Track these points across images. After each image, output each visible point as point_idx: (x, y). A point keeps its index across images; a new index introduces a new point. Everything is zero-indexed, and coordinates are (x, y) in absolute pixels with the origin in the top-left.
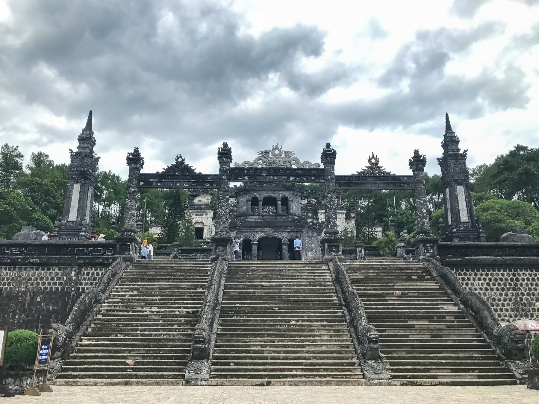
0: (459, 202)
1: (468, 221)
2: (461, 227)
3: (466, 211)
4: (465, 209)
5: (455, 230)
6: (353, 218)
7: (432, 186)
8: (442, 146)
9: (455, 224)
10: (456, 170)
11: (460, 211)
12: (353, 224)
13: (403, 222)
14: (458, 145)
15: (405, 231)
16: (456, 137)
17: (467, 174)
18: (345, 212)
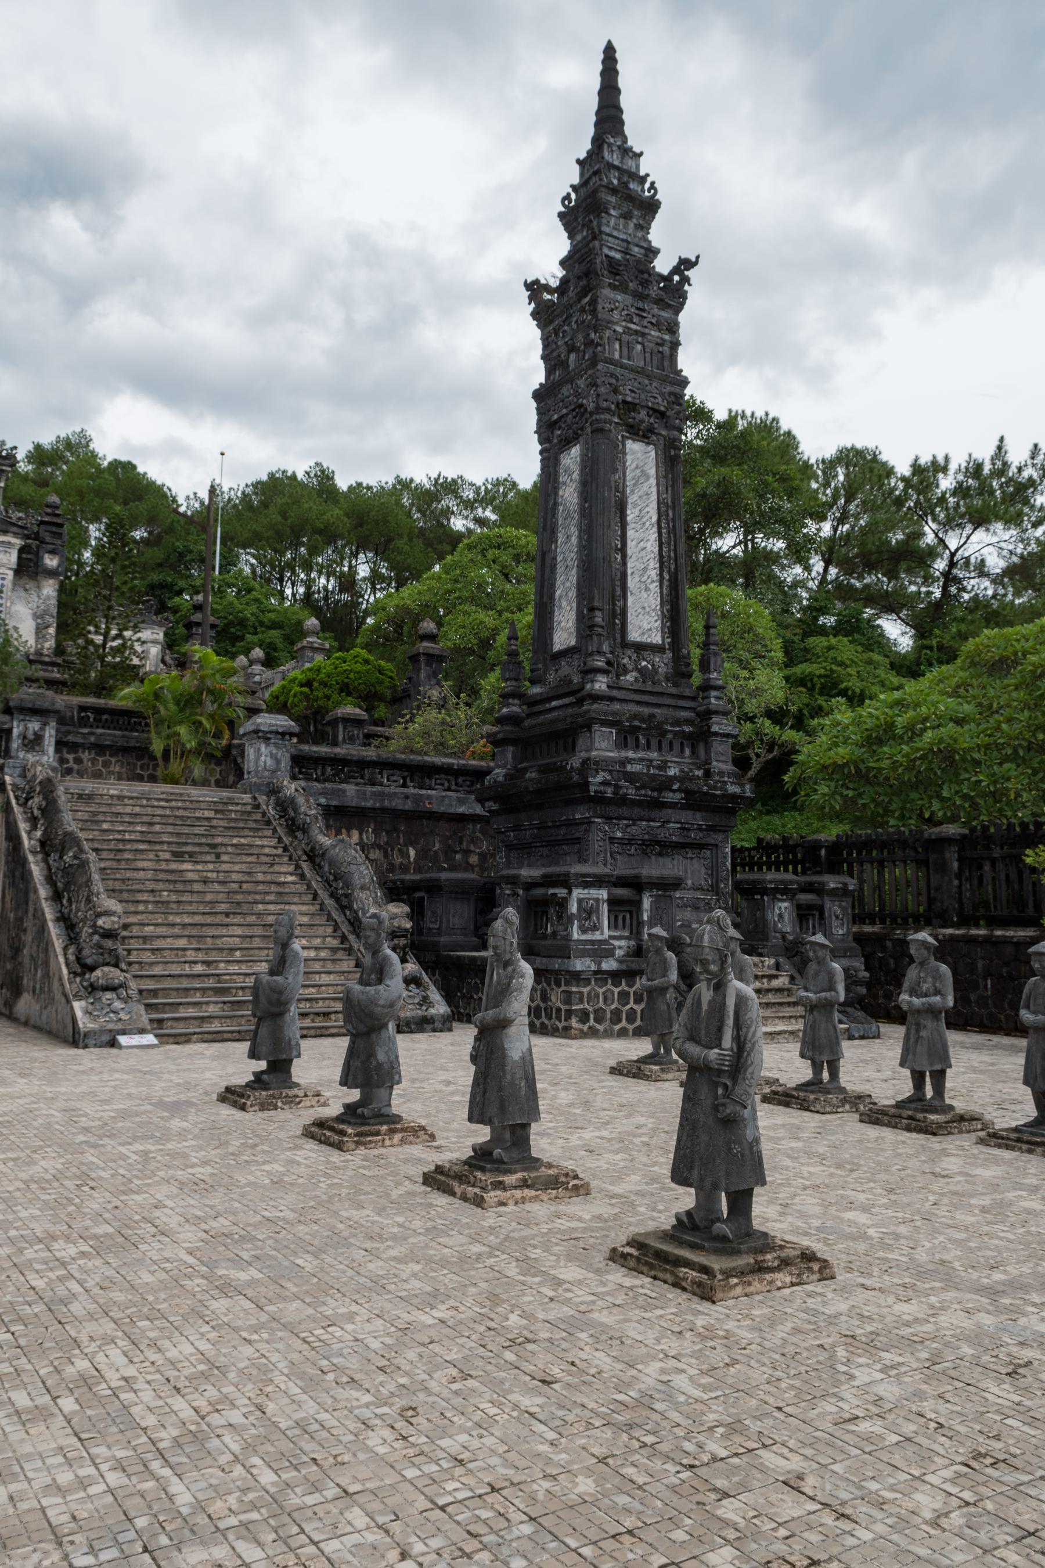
0: (630, 533)
1: (657, 639)
2: (626, 672)
3: (654, 587)
4: (654, 574)
5: (601, 684)
6: (52, 573)
7: (347, 515)
8: (561, 215)
9: (605, 647)
10: (630, 349)
11: (632, 583)
12: (48, 598)
13: (242, 623)
14: (645, 228)
15: (258, 653)
16: (643, 180)
17: (676, 389)
18: (18, 542)
